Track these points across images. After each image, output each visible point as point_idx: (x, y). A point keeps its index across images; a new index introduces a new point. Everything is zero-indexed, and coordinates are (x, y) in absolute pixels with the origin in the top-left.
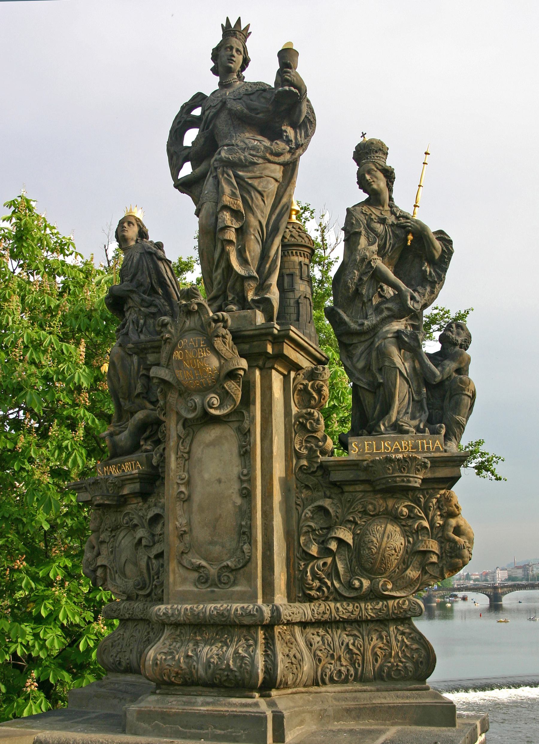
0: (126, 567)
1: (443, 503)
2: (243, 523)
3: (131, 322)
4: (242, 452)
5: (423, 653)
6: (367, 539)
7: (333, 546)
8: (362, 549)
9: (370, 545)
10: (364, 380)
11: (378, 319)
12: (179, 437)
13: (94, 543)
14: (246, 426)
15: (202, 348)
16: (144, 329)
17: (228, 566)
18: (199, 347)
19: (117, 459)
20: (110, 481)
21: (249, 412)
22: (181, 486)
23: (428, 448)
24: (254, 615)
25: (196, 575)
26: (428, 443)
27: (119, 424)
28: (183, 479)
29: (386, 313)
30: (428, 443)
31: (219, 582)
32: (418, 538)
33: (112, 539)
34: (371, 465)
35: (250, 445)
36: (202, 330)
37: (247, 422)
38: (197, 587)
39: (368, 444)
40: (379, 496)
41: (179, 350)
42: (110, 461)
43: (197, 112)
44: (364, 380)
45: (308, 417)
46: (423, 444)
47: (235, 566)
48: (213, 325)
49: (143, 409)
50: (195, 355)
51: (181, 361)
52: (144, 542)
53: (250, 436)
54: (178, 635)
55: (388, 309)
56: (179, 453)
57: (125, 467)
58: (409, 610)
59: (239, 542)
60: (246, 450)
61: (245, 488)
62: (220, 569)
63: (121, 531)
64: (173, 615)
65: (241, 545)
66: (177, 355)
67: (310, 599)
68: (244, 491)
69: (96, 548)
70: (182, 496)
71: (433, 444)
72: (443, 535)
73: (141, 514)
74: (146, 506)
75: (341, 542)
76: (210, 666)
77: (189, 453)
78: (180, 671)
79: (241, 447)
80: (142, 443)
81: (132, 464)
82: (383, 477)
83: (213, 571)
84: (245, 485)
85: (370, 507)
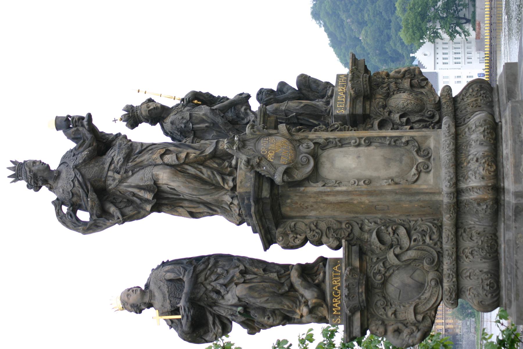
0: (416, 279)
1: (380, 76)
2: (388, 142)
3: (217, 282)
4: (340, 144)
5: (474, 86)
6: (402, 106)
7: (404, 119)
8: (407, 110)
9: (405, 104)
12: (324, 186)
13: (395, 326)
14: (322, 141)
15: (269, 139)
18: (268, 141)
19: (328, 298)
20: (348, 273)
22: (359, 184)
24: (449, 126)
25: (423, 175)
30: (342, 80)
31: (427, 156)
32: (402, 88)
33: (393, 306)
34: (354, 89)
35: (336, 138)
36: (255, 140)
37: (319, 140)
38: (430, 171)
40: (373, 100)
41: (268, 154)
42: (329, 305)
46: (341, 82)
47: (417, 147)
48: (255, 129)
49: (290, 278)
50: (273, 144)
51: (275, 153)
53: (329, 139)
54: (464, 178)
56: (336, 185)
57: (335, 285)
58: (448, 92)
59: (400, 147)
60: (339, 141)
61: (365, 141)
62: (419, 156)
63: (387, 293)
64: (449, 176)
65: (402, 145)
66: (270, 156)
67: (439, 122)
68: (367, 141)
69: (400, 326)
70: (366, 182)
72: (400, 79)
73: (375, 260)
74: (369, 253)
75: (401, 117)
76: (482, 144)
78: (487, 163)
79: (336, 146)
81: (335, 276)
82: (362, 86)
83: (420, 160)
84: (362, 142)
85: (381, 103)
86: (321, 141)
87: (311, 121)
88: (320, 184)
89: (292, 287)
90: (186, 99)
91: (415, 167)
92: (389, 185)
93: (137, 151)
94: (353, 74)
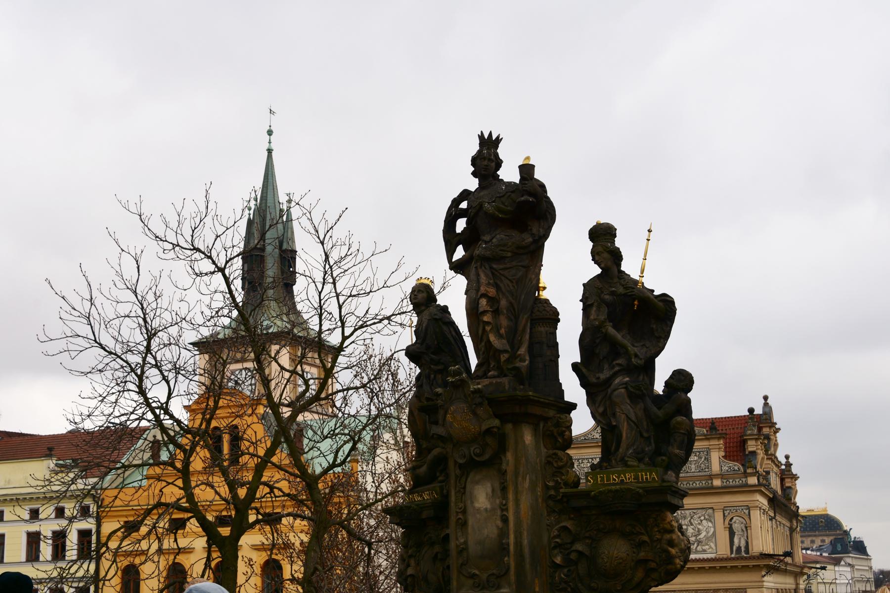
2: (504, 541)
7: (573, 556)
10: (604, 422)
11: (611, 373)
16: (434, 383)
17: (493, 574)
21: (505, 456)
23: (647, 479)
26: (646, 475)
27: (420, 459)
28: (460, 509)
29: (617, 368)
30: (646, 475)
39: (600, 477)
43: (464, 205)
44: (604, 422)
45: (554, 456)
46: (642, 475)
52: (439, 556)
55: (619, 365)
56: (457, 489)
61: (505, 515)
68: (504, 517)
70: (460, 521)
71: (650, 476)
75: (580, 553)
77: (464, 488)
80: (438, 474)
86: (504, 467)
87: (614, 444)
88: (458, 472)
89: (429, 451)
90: (634, 292)
91: (477, 572)
92: (457, 546)
93: (495, 266)
94: (623, 491)
